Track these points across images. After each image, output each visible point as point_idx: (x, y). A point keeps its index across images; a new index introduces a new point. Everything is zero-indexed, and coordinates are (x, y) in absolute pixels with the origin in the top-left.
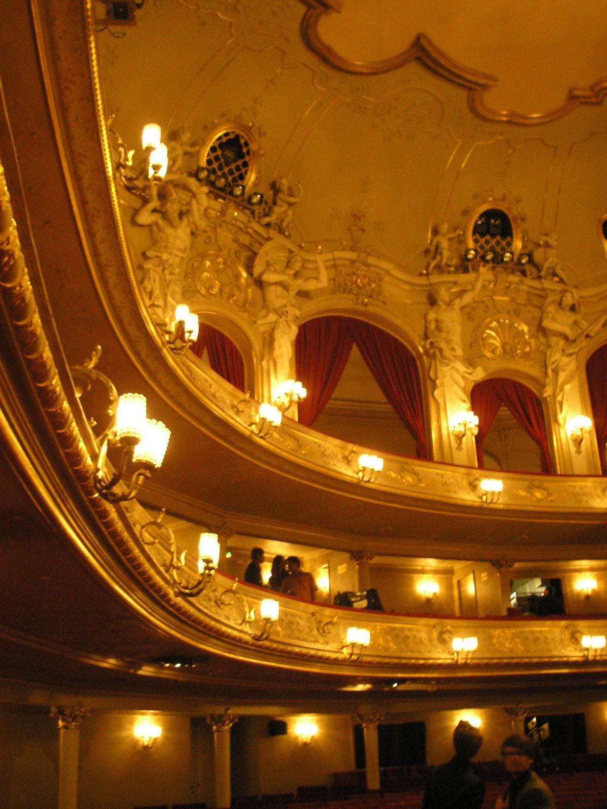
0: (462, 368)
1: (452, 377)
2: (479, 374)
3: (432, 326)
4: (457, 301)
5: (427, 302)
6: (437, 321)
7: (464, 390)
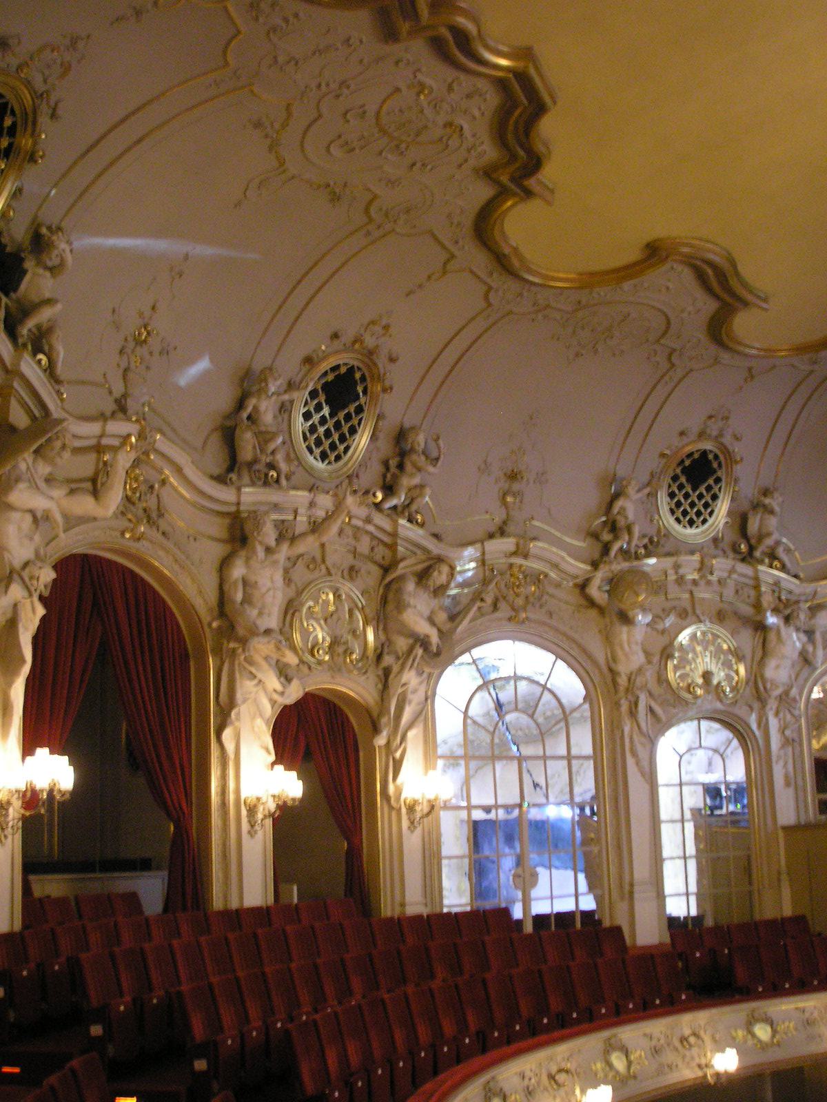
0: (273, 682)
1: (255, 700)
2: (294, 693)
3: (239, 596)
4: (285, 547)
5: (224, 534)
6: (245, 582)
7: (267, 723)
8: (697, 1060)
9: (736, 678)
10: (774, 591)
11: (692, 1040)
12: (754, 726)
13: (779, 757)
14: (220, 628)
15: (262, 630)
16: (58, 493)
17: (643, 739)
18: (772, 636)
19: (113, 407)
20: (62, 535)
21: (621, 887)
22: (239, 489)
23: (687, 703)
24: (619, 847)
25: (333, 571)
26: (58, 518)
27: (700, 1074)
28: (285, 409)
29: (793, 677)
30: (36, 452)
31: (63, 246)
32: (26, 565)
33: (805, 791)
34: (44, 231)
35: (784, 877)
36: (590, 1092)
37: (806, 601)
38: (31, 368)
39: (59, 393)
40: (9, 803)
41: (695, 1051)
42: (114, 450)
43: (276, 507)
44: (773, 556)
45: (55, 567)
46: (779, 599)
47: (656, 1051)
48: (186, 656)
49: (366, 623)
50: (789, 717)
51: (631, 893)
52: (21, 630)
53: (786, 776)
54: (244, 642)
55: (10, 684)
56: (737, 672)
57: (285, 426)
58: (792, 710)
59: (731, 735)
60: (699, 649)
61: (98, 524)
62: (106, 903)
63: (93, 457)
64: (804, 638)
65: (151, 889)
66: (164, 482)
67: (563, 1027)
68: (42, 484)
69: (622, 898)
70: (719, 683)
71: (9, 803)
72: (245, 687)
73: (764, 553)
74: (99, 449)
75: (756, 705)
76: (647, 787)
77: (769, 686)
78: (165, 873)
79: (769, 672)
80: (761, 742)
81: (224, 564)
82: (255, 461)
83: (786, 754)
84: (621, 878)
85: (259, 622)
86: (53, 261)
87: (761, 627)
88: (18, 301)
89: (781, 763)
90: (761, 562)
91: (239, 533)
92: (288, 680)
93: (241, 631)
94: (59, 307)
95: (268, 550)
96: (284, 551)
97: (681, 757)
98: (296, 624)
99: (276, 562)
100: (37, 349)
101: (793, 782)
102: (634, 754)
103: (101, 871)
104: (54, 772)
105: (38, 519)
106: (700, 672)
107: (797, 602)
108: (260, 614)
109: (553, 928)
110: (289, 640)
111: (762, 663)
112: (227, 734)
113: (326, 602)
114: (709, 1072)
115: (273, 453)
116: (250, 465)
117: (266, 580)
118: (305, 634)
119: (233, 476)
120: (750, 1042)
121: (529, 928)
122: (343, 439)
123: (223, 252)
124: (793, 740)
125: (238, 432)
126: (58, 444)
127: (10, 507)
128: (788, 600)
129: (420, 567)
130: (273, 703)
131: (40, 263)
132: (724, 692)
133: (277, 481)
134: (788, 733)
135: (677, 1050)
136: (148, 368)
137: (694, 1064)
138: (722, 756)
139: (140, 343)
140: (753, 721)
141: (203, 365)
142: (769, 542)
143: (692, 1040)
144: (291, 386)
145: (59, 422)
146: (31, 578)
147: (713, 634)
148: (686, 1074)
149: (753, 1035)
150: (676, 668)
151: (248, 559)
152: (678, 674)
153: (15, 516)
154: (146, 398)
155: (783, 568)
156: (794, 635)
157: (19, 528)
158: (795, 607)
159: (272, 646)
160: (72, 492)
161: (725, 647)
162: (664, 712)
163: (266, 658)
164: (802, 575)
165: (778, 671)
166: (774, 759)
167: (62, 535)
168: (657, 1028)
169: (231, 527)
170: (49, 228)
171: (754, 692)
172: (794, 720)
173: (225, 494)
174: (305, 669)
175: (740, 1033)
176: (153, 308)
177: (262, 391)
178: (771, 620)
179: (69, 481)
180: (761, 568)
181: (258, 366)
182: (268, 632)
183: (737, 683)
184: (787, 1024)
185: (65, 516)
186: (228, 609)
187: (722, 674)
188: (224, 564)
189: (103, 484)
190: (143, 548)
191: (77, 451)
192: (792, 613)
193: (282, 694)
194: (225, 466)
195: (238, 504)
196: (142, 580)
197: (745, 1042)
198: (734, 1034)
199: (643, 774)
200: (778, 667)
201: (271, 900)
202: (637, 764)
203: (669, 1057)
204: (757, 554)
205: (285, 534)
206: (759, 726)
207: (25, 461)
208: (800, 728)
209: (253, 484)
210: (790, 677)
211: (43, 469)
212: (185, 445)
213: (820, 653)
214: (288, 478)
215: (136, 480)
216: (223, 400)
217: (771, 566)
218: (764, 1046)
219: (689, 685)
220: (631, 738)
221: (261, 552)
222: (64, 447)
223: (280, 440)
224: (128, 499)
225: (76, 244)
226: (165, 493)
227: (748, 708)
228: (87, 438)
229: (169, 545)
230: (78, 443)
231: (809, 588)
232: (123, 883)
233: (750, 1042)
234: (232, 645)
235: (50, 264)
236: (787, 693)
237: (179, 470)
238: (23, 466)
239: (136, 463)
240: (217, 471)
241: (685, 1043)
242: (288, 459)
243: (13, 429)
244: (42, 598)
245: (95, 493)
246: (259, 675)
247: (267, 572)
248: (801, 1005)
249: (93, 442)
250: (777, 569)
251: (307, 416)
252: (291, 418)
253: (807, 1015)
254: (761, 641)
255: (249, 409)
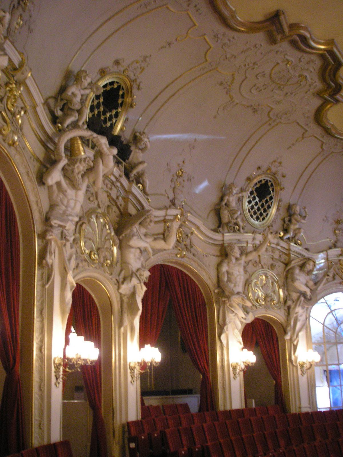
1: (234, 322)
2: (250, 318)
3: (225, 279)
4: (244, 257)
5: (218, 254)
6: (228, 273)
7: (239, 331)
14: (218, 293)
15: (236, 292)
16: (150, 240)
19: (170, 203)
20: (152, 257)
22: (223, 234)
25: (264, 267)
26: (150, 250)
28: (240, 200)
30: (140, 224)
31: (146, 140)
32: (138, 270)
34: (138, 134)
38: (136, 190)
39: (148, 199)
40: (135, 367)
42: (172, 221)
43: (239, 241)
45: (150, 271)
48: (204, 304)
49: (279, 287)
52: (137, 296)
54: (228, 298)
55: (133, 319)
57: (240, 207)
61: (166, 252)
62: (175, 408)
63: (162, 225)
65: (193, 402)
66: (192, 233)
68: (143, 237)
71: (135, 367)
72: (230, 317)
74: (165, 221)
78: (199, 395)
81: (219, 266)
82: (229, 222)
85: (234, 289)
86: (142, 146)
88: (129, 163)
91: (224, 253)
92: (248, 313)
93: (227, 293)
94: (146, 164)
95: (237, 259)
96: (244, 259)
98: (250, 289)
99: (240, 264)
100: (138, 182)
103: (172, 394)
104: (153, 354)
105: (142, 251)
108: (235, 286)
110: (247, 296)
112: (223, 337)
113: (262, 280)
115: (236, 219)
116: (227, 224)
117: (236, 271)
118: (254, 293)
119: (221, 229)
122: (265, 211)
123: (211, 137)
125: (221, 211)
126: (148, 220)
127: (130, 247)
129: (300, 263)
130: (242, 322)
131: (137, 147)
133: (239, 230)
136: (183, 187)
139: (179, 177)
141: (205, 184)
144: (242, 190)
145: (149, 211)
146: (140, 275)
151: (228, 263)
153: (133, 250)
154: (183, 199)
157: (135, 256)
159: (240, 299)
160: (155, 239)
163: (238, 304)
167: (152, 257)
169: (221, 250)
170: (140, 133)
173: (218, 237)
174: (254, 308)
176: (184, 162)
177: (230, 193)
179: (153, 235)
181: (228, 183)
182: (238, 293)
185: (153, 249)
186: (221, 285)
188: (219, 266)
189: (168, 235)
190: (185, 261)
191: (156, 222)
193: (245, 319)
194: (217, 225)
195: (223, 241)
196: (185, 274)
201: (244, 406)
205: (243, 252)
207: (136, 228)
209: (229, 232)
211: (143, 231)
212: (200, 217)
214: (243, 229)
215: (181, 233)
216: (214, 198)
221: (234, 260)
222: (151, 221)
223: (239, 213)
224: (178, 241)
225: (151, 139)
226: (193, 238)
228: (161, 217)
229: (196, 259)
230: (156, 219)
232: (182, 399)
234: (224, 299)
235: (141, 147)
237: (198, 228)
238: (135, 230)
239: (181, 226)
240: (213, 227)
242: (243, 220)
243: (130, 215)
244: (145, 284)
245: (164, 239)
246: (235, 311)
247: (237, 268)
249: (162, 218)
251: (250, 202)
252: (243, 203)
255: (225, 201)
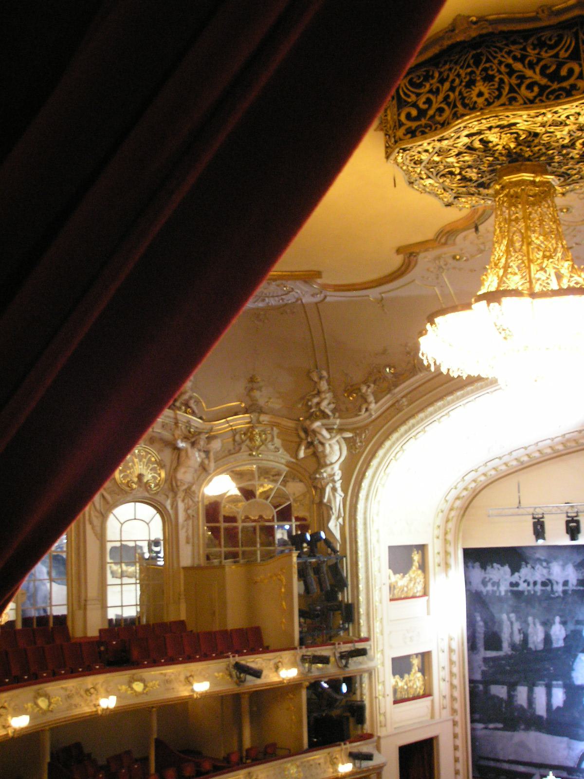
8: (94, 703)
9: (159, 478)
10: (187, 427)
11: (92, 691)
12: (169, 508)
13: (183, 527)
17: (97, 514)
18: (183, 454)
21: (79, 601)
23: (126, 492)
24: (79, 579)
27: (94, 709)
29: (196, 479)
33: (199, 546)
35: (182, 597)
36: (15, 719)
37: (207, 433)
41: (94, 696)
44: (187, 405)
46: (190, 432)
47: (69, 697)
50: (191, 503)
51: (85, 605)
53: (187, 538)
56: (160, 476)
58: (193, 499)
59: (154, 511)
60: (136, 460)
64: (203, 455)
67: (18, 682)
69: (80, 608)
70: (148, 481)
73: (182, 404)
75: (171, 495)
76: (98, 542)
77: (179, 484)
79: (180, 475)
80: (173, 517)
83: (188, 525)
84: (79, 597)
87: (176, 448)
89: (185, 530)
90: (179, 409)
97: (122, 524)
101: (191, 540)
102: (91, 523)
106: (136, 473)
107: (200, 433)
109: (35, 626)
111: (176, 470)
114: (100, 709)
120: (129, 692)
121: (19, 626)
124: (193, 516)
128: (195, 432)
132: (150, 486)
134: (190, 512)
135: (82, 696)
137: (91, 704)
138: (148, 524)
140: (168, 504)
142: (186, 397)
143: (92, 691)
147: (146, 451)
148: (86, 709)
149: (132, 689)
150: (121, 472)
152: (122, 475)
155: (193, 413)
156: (197, 454)
158: (197, 437)
161: (153, 459)
162: (112, 497)
164: (204, 418)
165: (185, 475)
166: (180, 527)
168: (71, 684)
171: (170, 487)
172: (194, 505)
175: (124, 687)
178: (181, 444)
180: (178, 412)
183: (159, 481)
184: (154, 682)
187: (150, 476)
192: (196, 440)
197: (126, 691)
198: (120, 688)
199: (96, 535)
200: (185, 472)
202: (93, 527)
203: (77, 700)
204: (178, 404)
206: (172, 506)
208: (198, 508)
210: (194, 478)
213: (212, 465)
217: (186, 412)
218: (137, 694)
219: (128, 482)
220: (90, 513)
227: (165, 497)
231: (208, 425)
233: (129, 692)
236: (189, 488)
241: (88, 693)
248: (164, 672)
250: (190, 414)
253: (167, 677)
254: (177, 456)
